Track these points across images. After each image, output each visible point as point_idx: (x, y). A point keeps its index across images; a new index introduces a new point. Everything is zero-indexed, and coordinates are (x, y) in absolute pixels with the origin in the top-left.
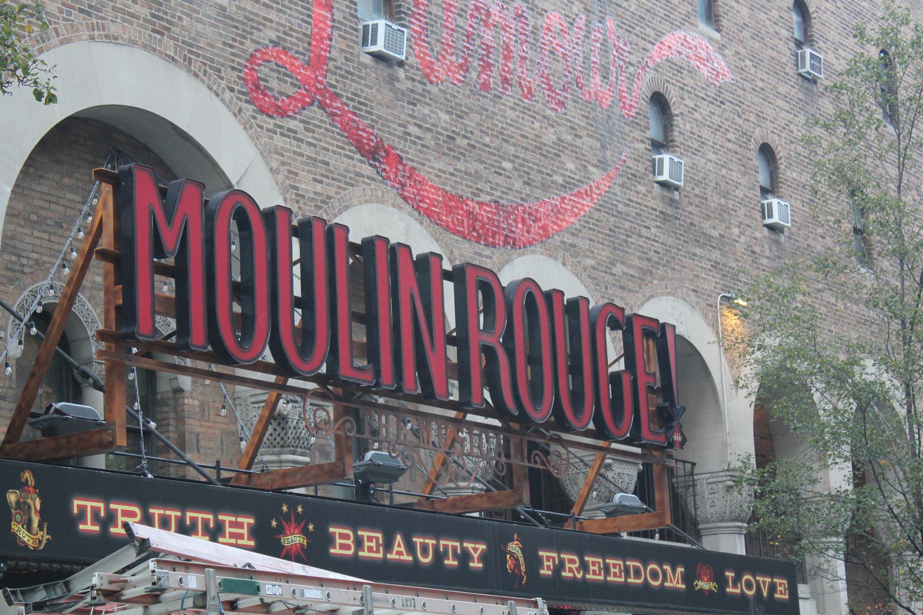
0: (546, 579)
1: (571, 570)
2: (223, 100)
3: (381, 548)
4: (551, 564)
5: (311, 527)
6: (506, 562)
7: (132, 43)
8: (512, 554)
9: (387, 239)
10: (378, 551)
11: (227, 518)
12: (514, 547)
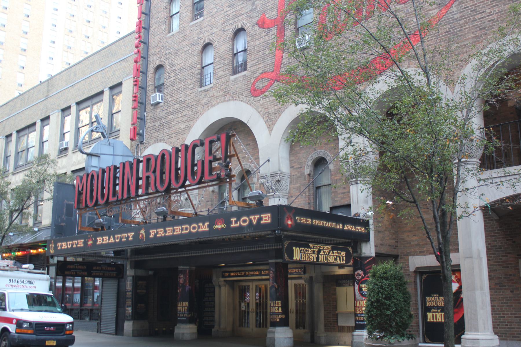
0: (152, 238)
1: (160, 234)
2: (243, 102)
7: (219, 103)
11: (79, 241)
12: (142, 232)
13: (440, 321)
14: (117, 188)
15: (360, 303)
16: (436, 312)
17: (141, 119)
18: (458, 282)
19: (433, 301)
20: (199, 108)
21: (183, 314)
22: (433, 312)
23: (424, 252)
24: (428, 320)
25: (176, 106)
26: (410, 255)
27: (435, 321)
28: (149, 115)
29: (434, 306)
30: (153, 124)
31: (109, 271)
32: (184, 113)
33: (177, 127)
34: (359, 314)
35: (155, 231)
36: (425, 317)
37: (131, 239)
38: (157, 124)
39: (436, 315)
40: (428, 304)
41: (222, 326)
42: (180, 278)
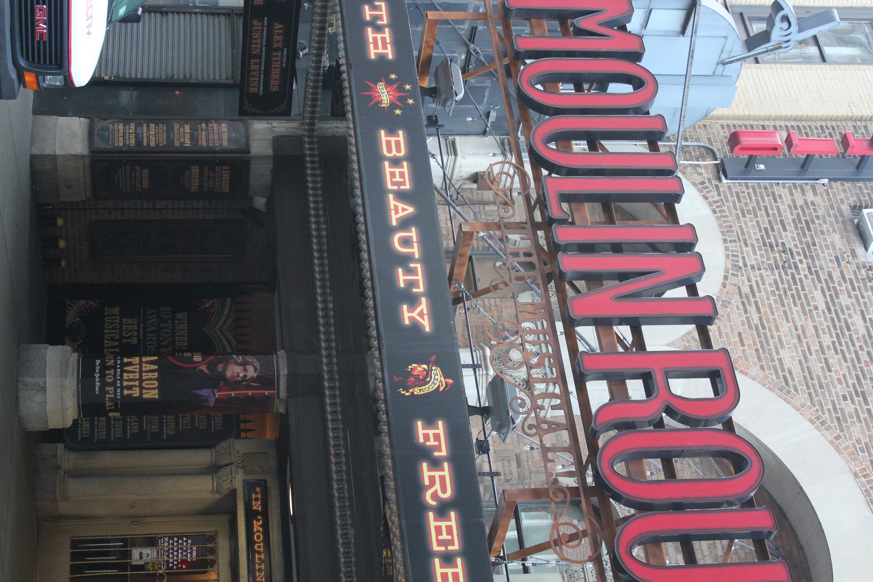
3: (396, 188)
4: (432, 443)
5: (398, 112)
6: (420, 363)
8: (428, 372)
9: (704, 269)
10: (393, 183)
14: (566, 88)
17: (806, 167)
20: (857, 431)
21: (113, 384)
25: (857, 319)
28: (818, 200)
30: (788, 217)
31: (267, 73)
32: (834, 360)
33: (785, 327)
35: (444, 453)
37: (407, 315)
38: (789, 238)
41: (74, 487)
42: (244, 364)
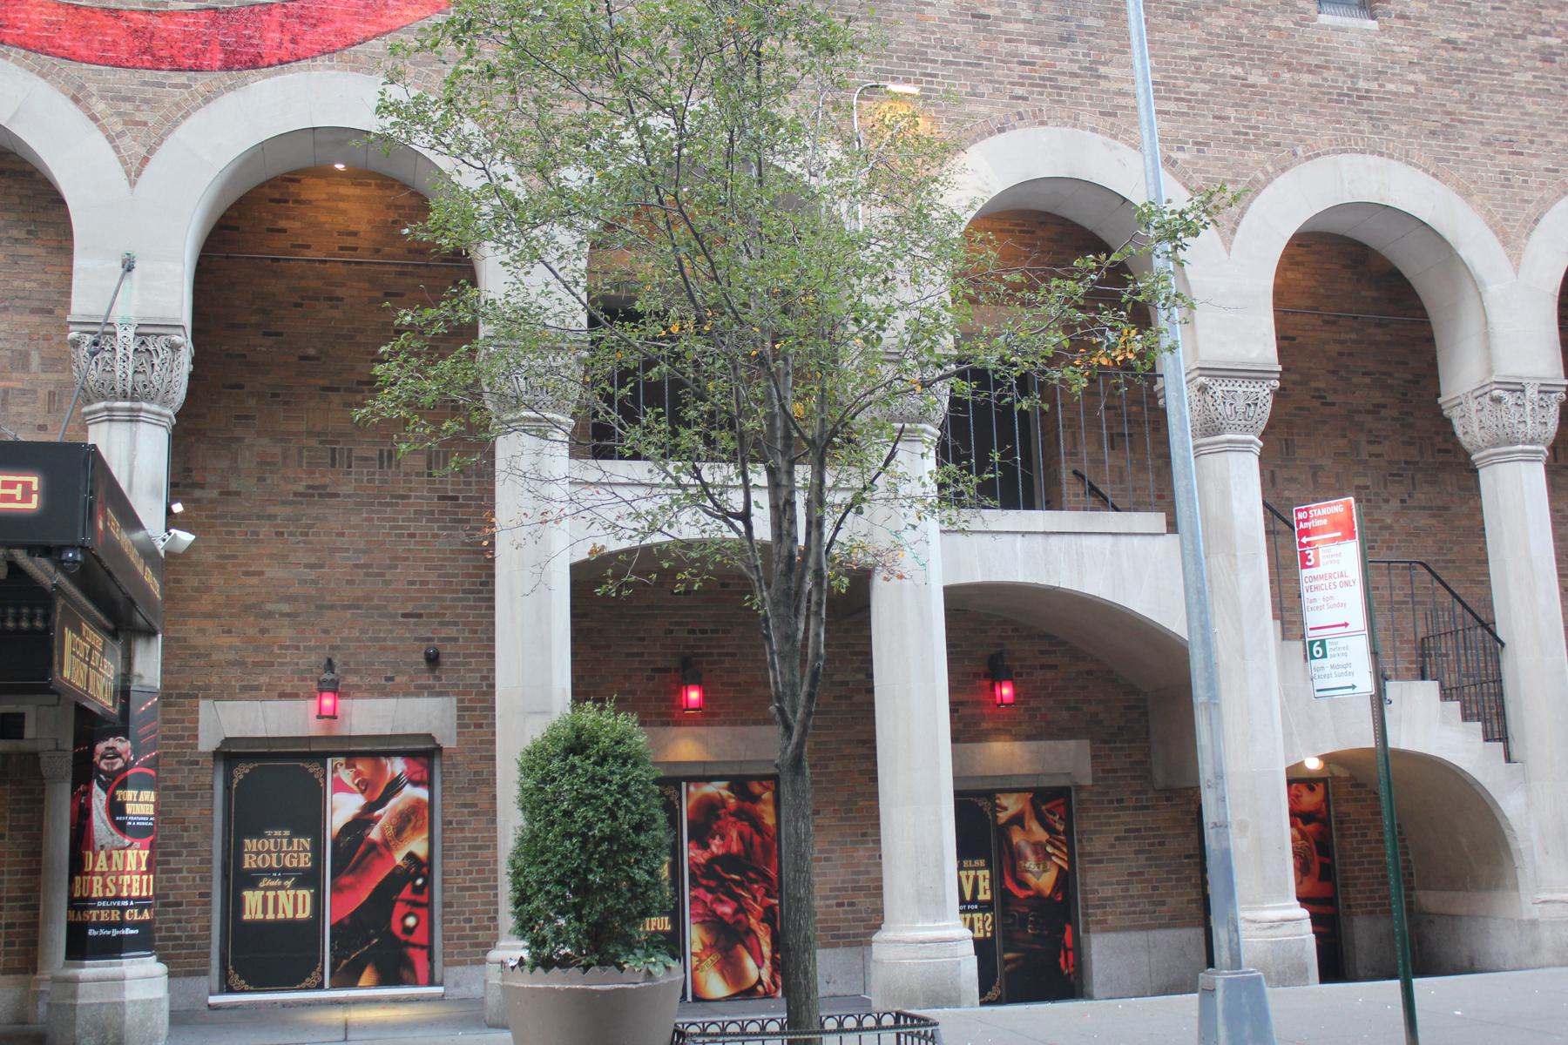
13: (290, 915)
15: (109, 858)
16: (276, 888)
18: (363, 792)
19: (269, 852)
22: (267, 889)
23: (257, 688)
24: (247, 917)
26: (206, 697)
27: (270, 916)
29: (270, 870)
34: (104, 899)
36: (233, 905)
39: (276, 898)
40: (249, 862)
